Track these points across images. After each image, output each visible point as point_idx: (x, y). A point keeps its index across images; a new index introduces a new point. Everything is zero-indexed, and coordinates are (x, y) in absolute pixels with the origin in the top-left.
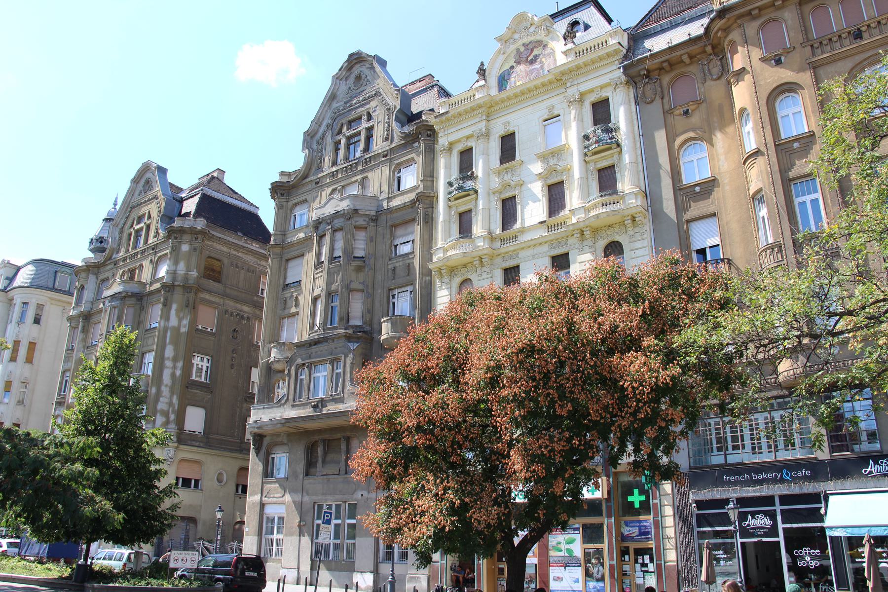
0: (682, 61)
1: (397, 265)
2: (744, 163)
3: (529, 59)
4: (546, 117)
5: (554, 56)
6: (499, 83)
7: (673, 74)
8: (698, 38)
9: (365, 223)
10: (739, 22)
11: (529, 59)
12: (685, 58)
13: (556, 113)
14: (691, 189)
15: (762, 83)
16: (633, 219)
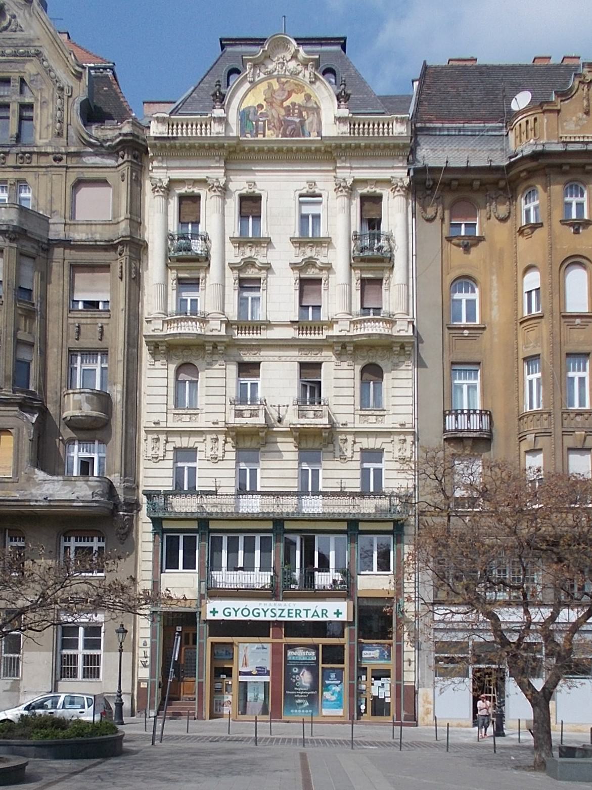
0: (471, 185)
1: (83, 321)
2: (521, 323)
3: (285, 104)
4: (304, 191)
5: (319, 114)
6: (241, 120)
7: (457, 195)
8: (498, 169)
9: (34, 251)
10: (547, 170)
11: (285, 104)
12: (477, 184)
13: (317, 191)
14: (460, 331)
15: (558, 247)
16: (402, 347)
